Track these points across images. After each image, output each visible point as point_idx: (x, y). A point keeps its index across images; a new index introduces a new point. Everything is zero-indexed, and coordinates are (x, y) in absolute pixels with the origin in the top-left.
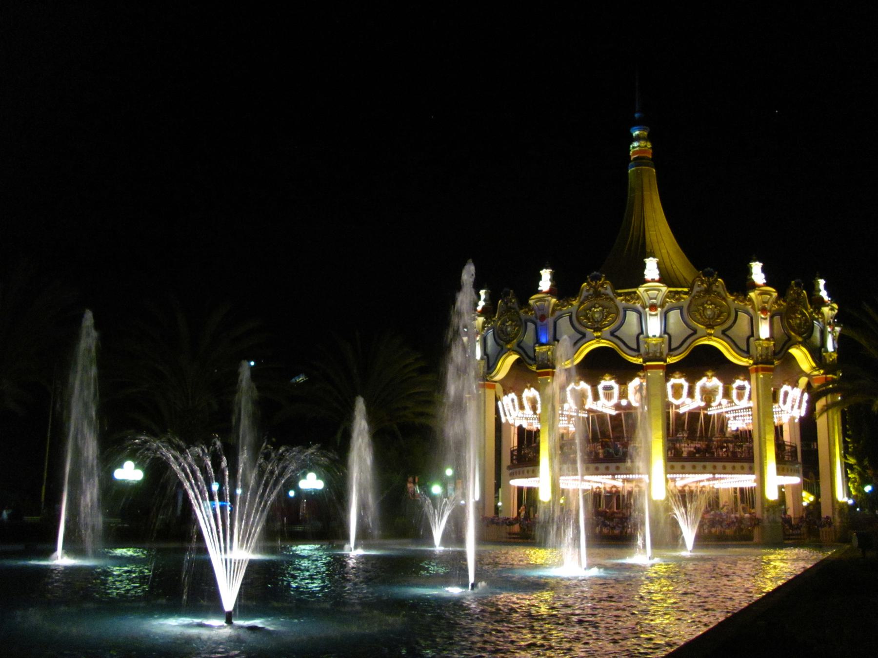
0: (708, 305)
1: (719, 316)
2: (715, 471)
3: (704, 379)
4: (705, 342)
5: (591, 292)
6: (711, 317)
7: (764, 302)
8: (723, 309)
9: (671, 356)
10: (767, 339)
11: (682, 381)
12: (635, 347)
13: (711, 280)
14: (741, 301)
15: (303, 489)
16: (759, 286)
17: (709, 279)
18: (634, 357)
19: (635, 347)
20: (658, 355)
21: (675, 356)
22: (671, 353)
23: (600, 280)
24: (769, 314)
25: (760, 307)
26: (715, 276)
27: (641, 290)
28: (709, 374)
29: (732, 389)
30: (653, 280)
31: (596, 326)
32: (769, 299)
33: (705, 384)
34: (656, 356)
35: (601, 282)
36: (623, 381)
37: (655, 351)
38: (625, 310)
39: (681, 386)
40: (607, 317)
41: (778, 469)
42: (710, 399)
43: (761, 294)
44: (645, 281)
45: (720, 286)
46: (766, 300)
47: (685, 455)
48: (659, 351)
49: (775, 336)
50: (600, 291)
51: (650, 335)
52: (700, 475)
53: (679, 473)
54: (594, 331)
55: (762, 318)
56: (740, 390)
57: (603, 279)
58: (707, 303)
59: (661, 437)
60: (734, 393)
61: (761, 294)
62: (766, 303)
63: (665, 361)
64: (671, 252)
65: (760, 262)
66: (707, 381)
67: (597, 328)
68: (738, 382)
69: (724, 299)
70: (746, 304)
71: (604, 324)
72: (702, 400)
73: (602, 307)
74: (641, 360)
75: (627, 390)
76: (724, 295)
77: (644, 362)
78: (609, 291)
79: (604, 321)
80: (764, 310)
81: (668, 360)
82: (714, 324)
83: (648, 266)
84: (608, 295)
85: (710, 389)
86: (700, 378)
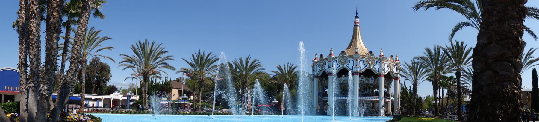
69: (347, 58)
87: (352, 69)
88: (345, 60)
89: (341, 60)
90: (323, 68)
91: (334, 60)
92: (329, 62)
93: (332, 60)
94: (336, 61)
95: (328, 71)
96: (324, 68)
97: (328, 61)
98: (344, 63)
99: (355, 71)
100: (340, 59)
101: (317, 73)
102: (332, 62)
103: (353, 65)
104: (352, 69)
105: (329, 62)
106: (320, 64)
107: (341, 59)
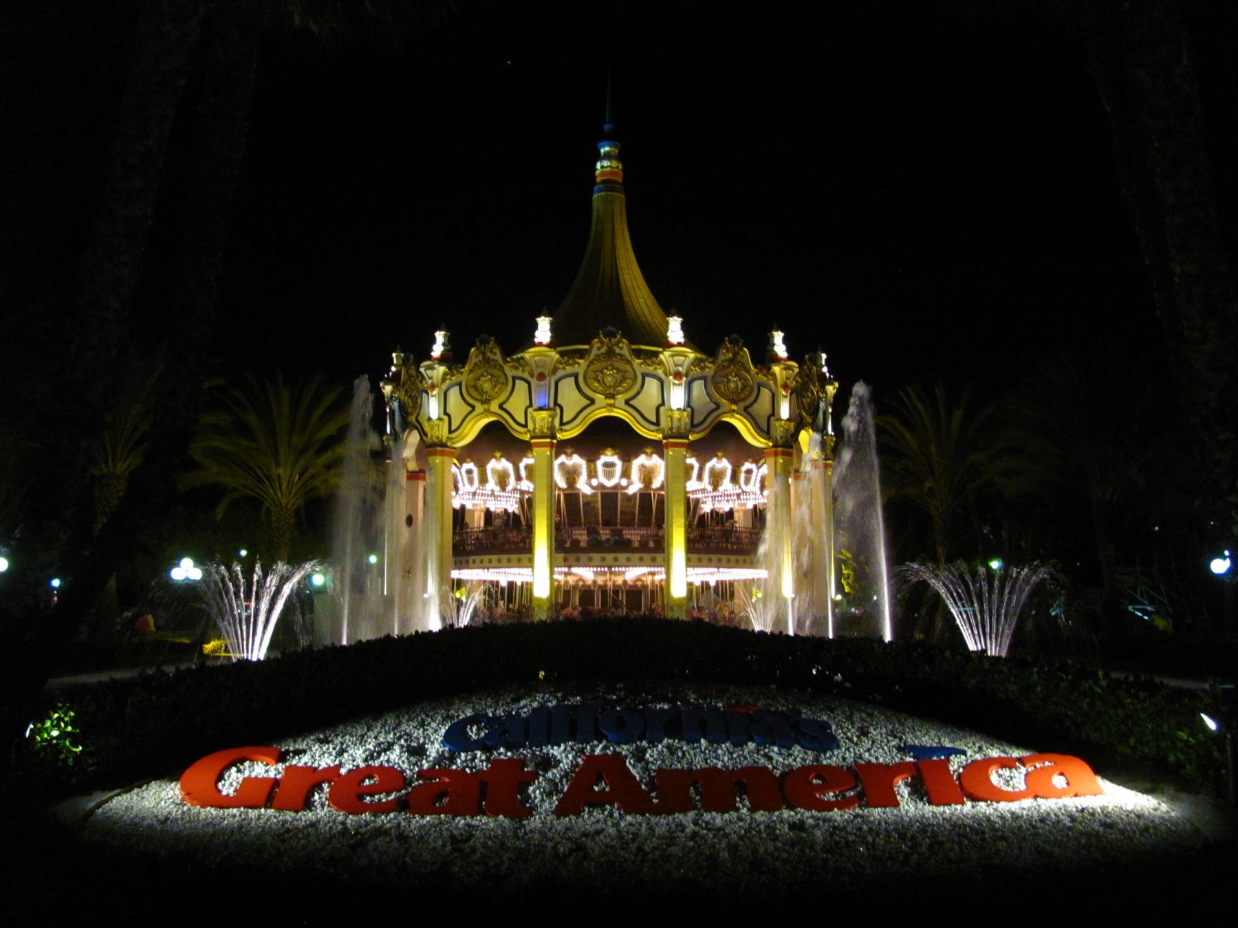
0: (608, 370)
1: (621, 382)
2: (629, 564)
3: (715, 460)
4: (604, 413)
5: (481, 358)
6: (612, 384)
7: (676, 365)
8: (627, 375)
9: (562, 430)
10: (679, 409)
11: (615, 459)
12: (523, 422)
13: (613, 340)
14: (649, 365)
15: (177, 581)
16: (672, 345)
17: (610, 340)
18: (653, 431)
19: (523, 422)
20: (545, 430)
21: (697, 433)
22: (564, 428)
23: (615, 337)
24: (684, 378)
25: (672, 371)
26: (618, 336)
27: (529, 354)
28: (720, 454)
29: (740, 472)
30: (540, 344)
31: (608, 392)
32: (684, 361)
33: (714, 465)
34: (543, 432)
35: (616, 340)
36: (627, 458)
37: (541, 426)
38: (514, 379)
39: (692, 467)
40: (495, 386)
41: (686, 564)
42: (718, 482)
43: (673, 356)
44: (534, 345)
45: (625, 348)
46: (680, 363)
47: (636, 544)
48: (546, 426)
49: (693, 404)
50: (614, 351)
51: (674, 407)
52: (638, 568)
53: (561, 567)
54: (606, 398)
55: (674, 384)
56: (606, 467)
57: (492, 343)
58: (607, 368)
59: (683, 525)
60: (742, 477)
61: (673, 356)
62: (681, 366)
63: (688, 438)
64: (648, 302)
65: (679, 317)
66: (717, 462)
67: (610, 394)
68: (641, 460)
69: (629, 362)
70: (656, 368)
71: (618, 391)
72: (710, 483)
73: (491, 375)
74: (661, 436)
75: (631, 468)
76: (630, 359)
77: (665, 438)
78: (498, 357)
79: (618, 387)
80: (678, 375)
81: (690, 437)
82: (615, 393)
83: (539, 327)
84: (497, 361)
85: (718, 471)
86: (636, 456)
87: (654, 419)
88: (625, 372)
89: (595, 372)
90: (494, 406)
91: (560, 373)
92: (534, 382)
93: (555, 370)
94: (576, 376)
95: (525, 426)
96: (501, 407)
97: (526, 376)
98: (615, 387)
99: (671, 429)
100: (592, 367)
101: (450, 432)
102: (553, 379)
103: (660, 402)
104: (654, 419)
105: (534, 382)
106: (475, 388)
107: (597, 366)
